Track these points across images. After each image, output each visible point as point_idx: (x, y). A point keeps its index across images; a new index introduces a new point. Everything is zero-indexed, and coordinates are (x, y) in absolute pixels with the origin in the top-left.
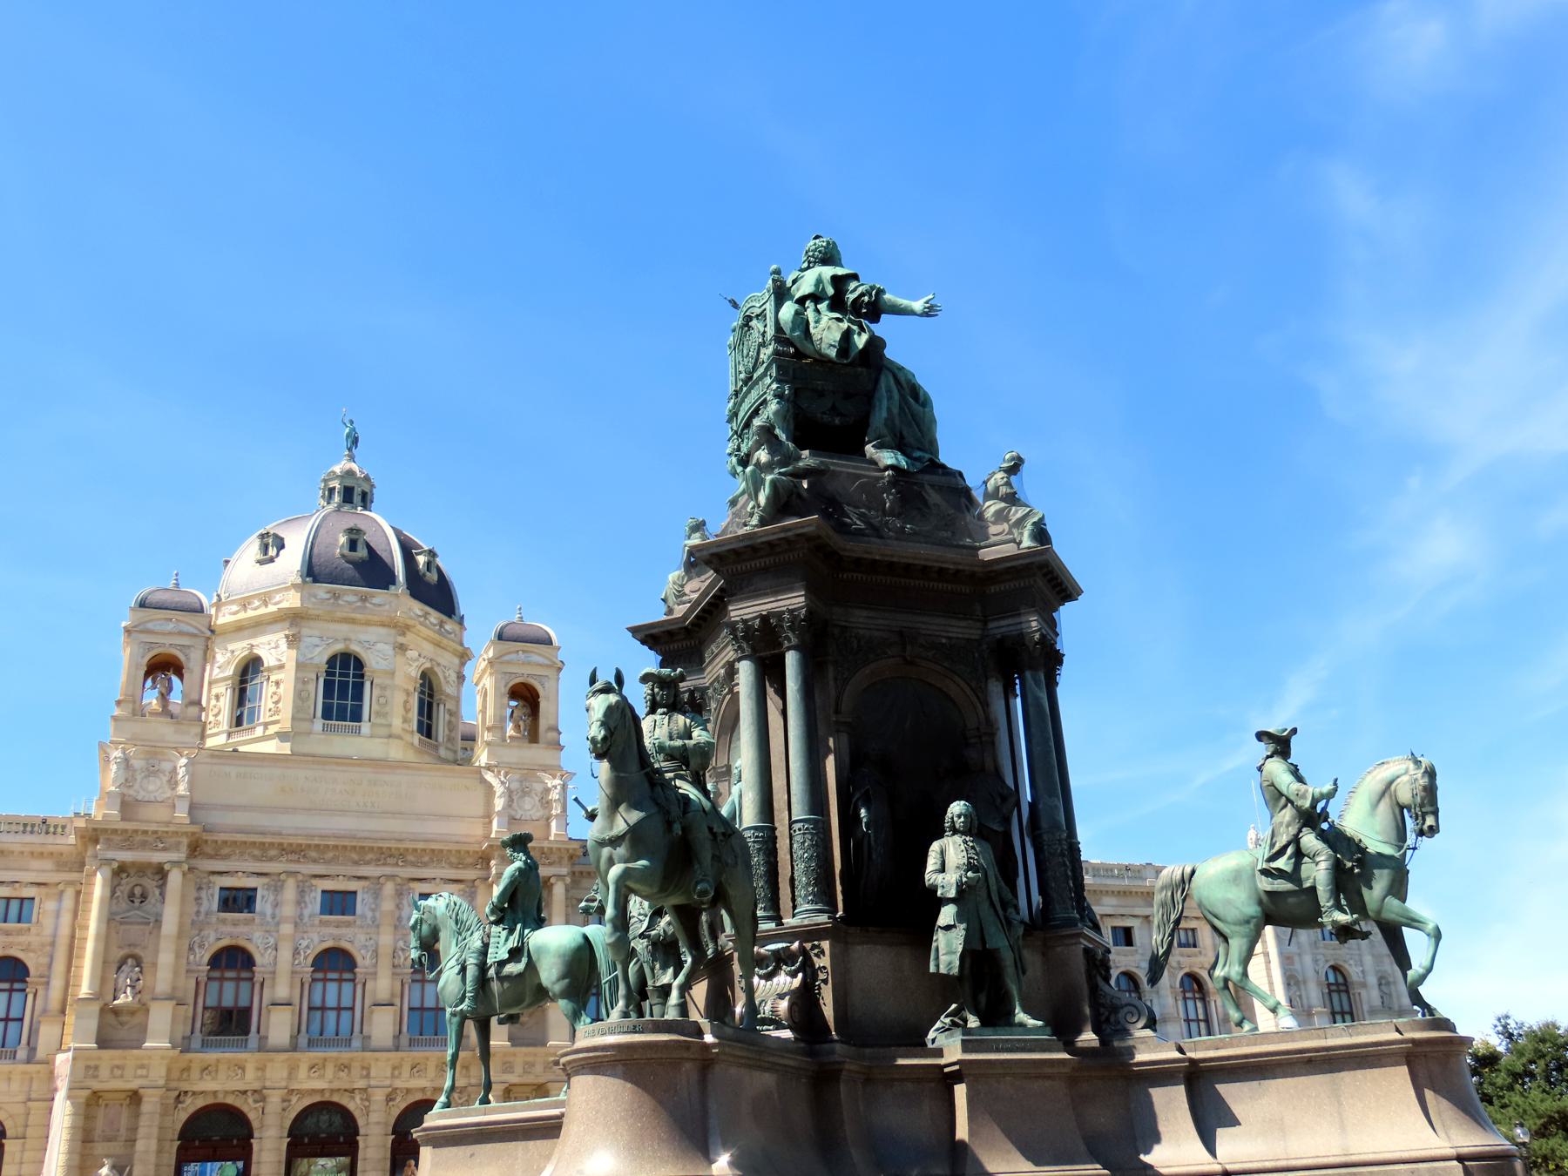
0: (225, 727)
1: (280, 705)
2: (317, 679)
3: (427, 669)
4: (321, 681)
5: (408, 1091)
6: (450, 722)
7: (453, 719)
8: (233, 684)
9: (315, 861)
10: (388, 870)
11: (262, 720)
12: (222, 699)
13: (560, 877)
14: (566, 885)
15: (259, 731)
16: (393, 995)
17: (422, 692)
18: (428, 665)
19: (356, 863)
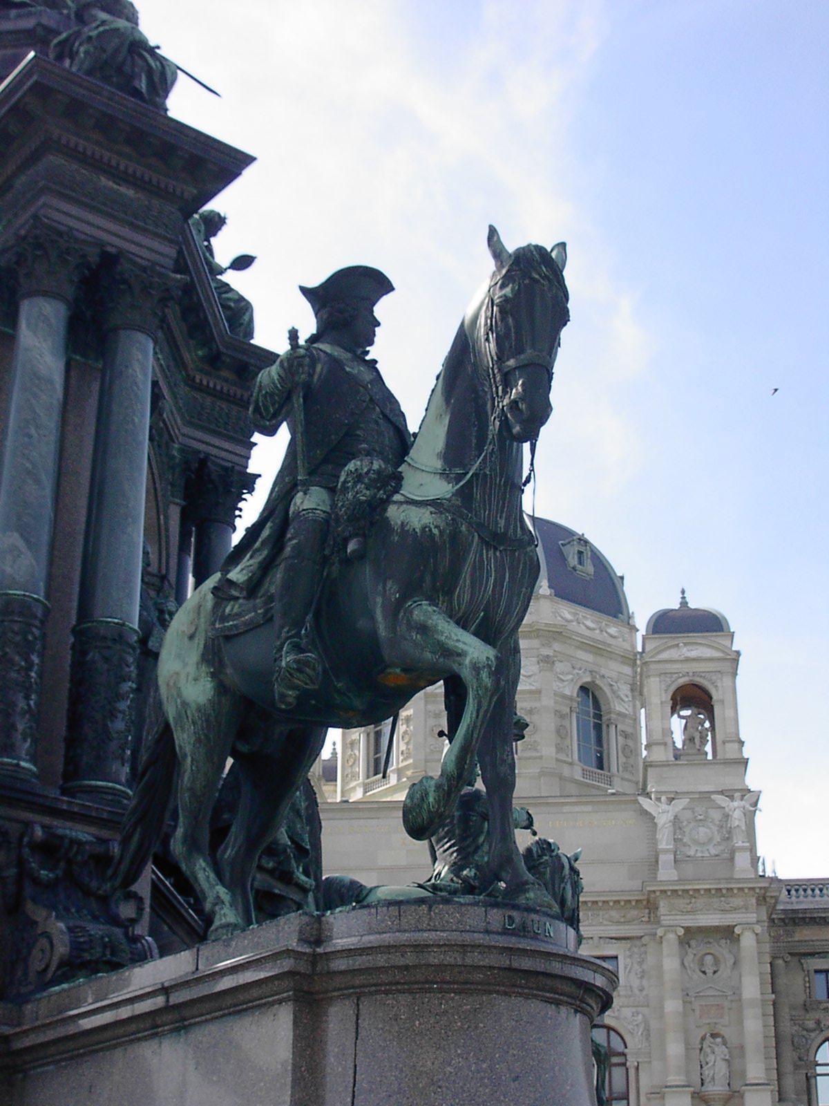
3: (587, 683)
6: (625, 747)
7: (630, 743)
13: (748, 925)
18: (588, 679)
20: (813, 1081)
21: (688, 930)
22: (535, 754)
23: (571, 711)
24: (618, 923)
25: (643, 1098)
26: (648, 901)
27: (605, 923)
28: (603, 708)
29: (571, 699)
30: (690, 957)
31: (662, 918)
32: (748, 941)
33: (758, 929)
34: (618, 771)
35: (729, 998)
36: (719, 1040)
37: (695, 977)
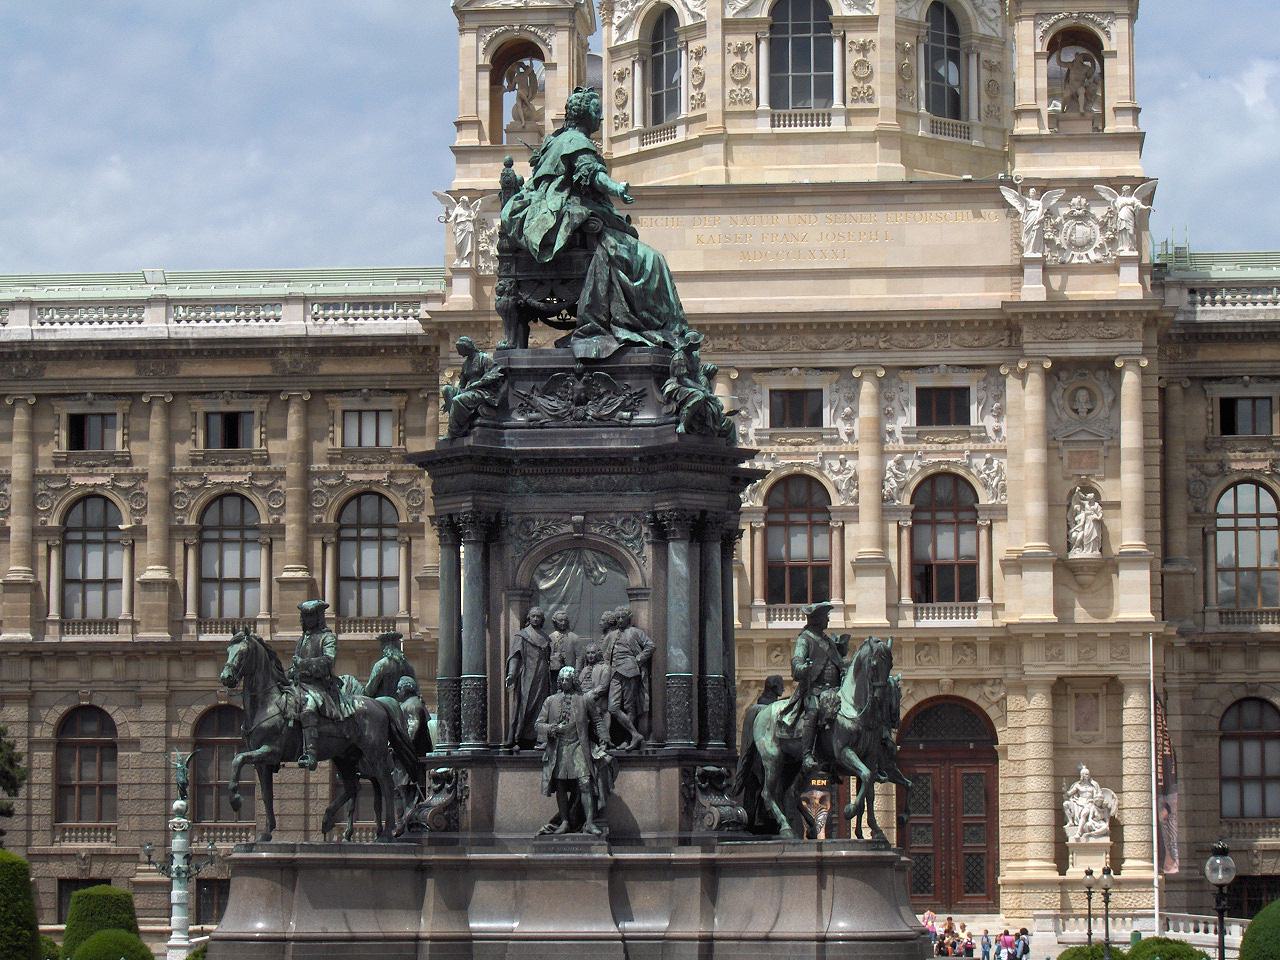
0: (638, 125)
1: (704, 90)
2: (758, 42)
4: (763, 46)
5: (917, 683)
7: (997, 77)
8: (641, 54)
9: (754, 350)
10: (862, 357)
11: (684, 112)
12: (628, 80)
14: (1144, 372)
15: (681, 135)
16: (883, 543)
17: (936, 38)
19: (816, 349)
20: (1211, 538)
21: (1056, 361)
22: (868, 106)
23: (918, 42)
24: (971, 348)
25: (996, 566)
26: (1009, 321)
27: (955, 347)
28: (962, 28)
29: (918, 25)
30: (1058, 393)
31: (1025, 346)
32: (1130, 380)
33: (1144, 363)
34: (979, 117)
35: (1105, 443)
36: (1091, 495)
37: (1065, 417)
